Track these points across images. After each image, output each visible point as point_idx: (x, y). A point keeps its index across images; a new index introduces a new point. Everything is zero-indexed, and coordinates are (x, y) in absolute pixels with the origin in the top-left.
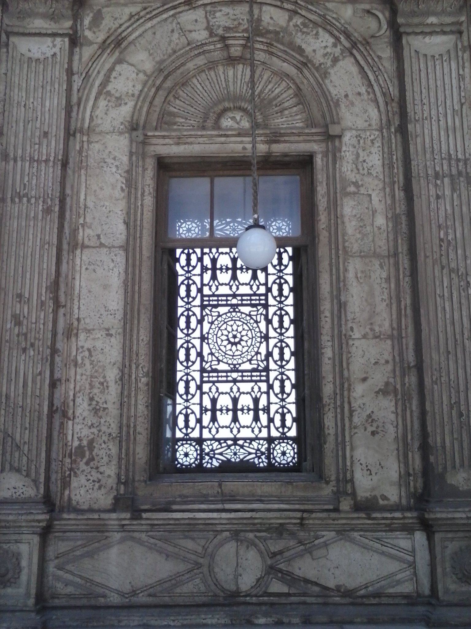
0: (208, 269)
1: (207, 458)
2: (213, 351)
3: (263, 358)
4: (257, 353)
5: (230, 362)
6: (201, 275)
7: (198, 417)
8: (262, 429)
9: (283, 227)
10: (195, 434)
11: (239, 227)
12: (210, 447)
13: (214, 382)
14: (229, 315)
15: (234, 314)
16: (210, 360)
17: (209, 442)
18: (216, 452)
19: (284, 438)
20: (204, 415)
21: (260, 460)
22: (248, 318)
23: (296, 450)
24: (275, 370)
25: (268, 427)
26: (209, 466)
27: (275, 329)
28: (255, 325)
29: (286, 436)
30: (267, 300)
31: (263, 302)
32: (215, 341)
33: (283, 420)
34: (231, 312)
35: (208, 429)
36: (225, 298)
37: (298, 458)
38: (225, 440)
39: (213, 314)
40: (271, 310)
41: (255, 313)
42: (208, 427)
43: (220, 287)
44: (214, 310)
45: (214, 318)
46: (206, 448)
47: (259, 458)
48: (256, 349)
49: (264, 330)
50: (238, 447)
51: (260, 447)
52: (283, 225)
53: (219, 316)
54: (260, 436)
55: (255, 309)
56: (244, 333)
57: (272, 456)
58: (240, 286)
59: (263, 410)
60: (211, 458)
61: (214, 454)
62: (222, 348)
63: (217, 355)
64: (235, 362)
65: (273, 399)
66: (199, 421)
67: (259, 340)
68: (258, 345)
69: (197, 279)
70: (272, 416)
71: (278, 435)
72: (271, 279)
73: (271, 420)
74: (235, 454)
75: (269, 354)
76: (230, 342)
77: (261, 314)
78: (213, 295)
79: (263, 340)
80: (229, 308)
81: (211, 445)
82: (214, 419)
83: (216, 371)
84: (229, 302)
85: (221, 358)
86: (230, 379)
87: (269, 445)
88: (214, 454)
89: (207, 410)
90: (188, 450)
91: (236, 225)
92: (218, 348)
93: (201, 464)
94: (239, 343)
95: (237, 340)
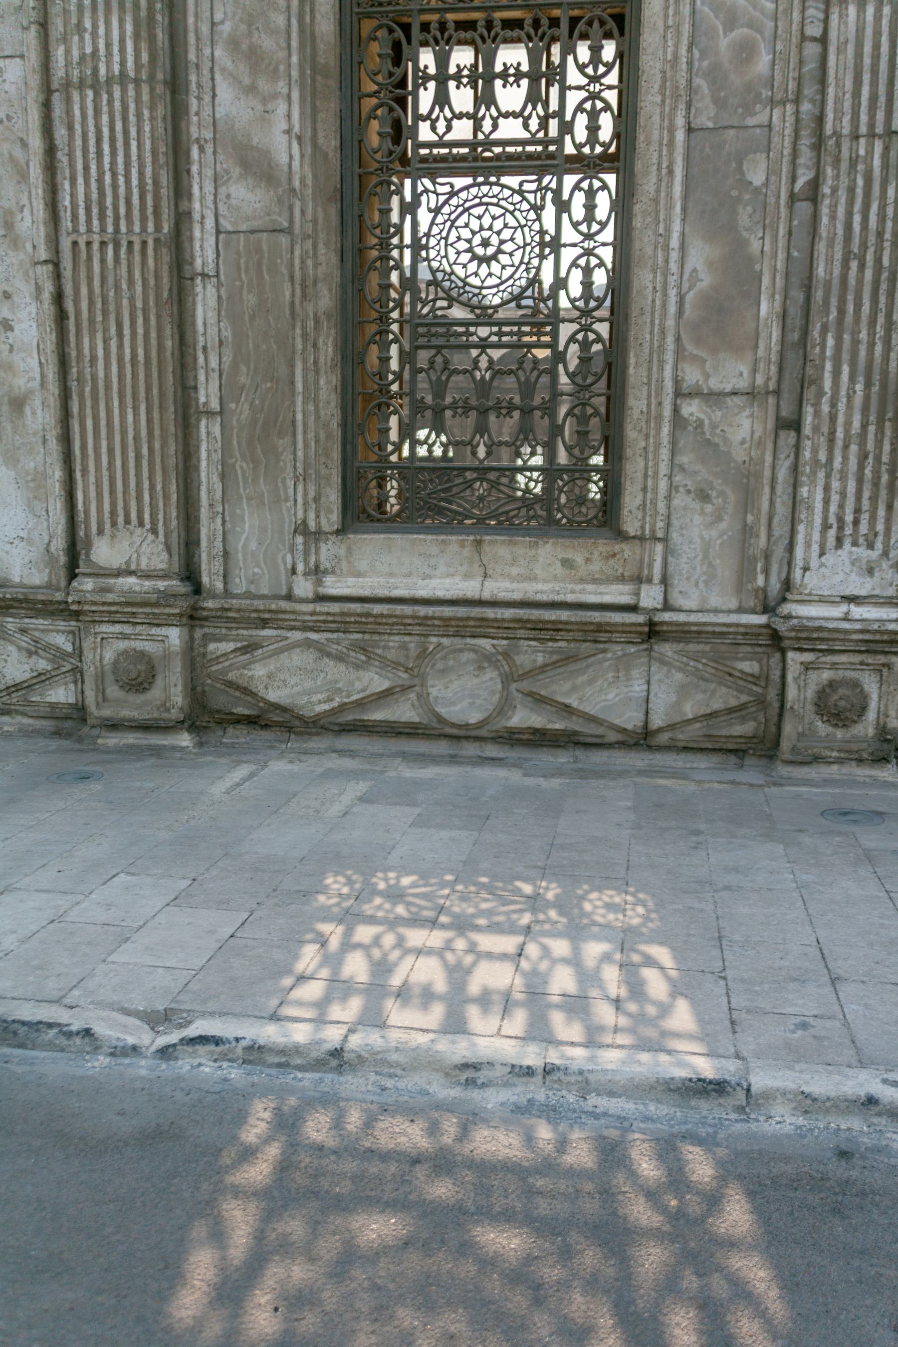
13: (439, 349)
15: (485, 189)
22: (517, 198)
28: (532, 215)
45: (442, 199)
56: (506, 234)
58: (501, 121)
68: (535, 262)
72: (573, 98)
78: (441, 144)
94: (494, 257)
95: (491, 251)
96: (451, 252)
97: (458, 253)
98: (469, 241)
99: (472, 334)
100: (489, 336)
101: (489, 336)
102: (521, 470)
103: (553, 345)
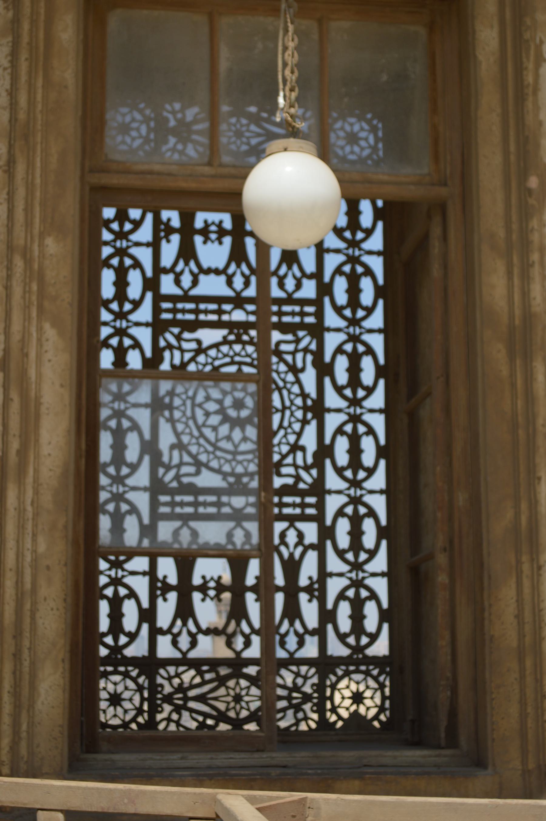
0: (173, 231)
1: (167, 708)
2: (185, 439)
3: (310, 460)
4: (295, 448)
5: (227, 468)
6: (155, 246)
7: (145, 604)
8: (307, 638)
9: (363, 134)
10: (138, 649)
11: (253, 128)
12: (176, 681)
13: (185, 519)
14: (225, 349)
15: (237, 348)
16: (176, 460)
17: (172, 670)
18: (192, 693)
19: (358, 661)
20: (160, 600)
21: (300, 715)
23: (387, 691)
24: (339, 492)
25: (320, 633)
26: (173, 727)
27: (339, 390)
28: (290, 377)
29: (366, 657)
30: (320, 314)
31: (310, 320)
32: (189, 413)
33: (357, 617)
34: (230, 343)
35: (169, 637)
36: (213, 307)
37: (391, 708)
38: (214, 663)
39: (186, 345)
40: (332, 341)
41: (291, 347)
42: (169, 631)
43: (202, 277)
44: (186, 335)
46: (166, 683)
47: (298, 708)
48: (292, 438)
49: (311, 388)
50: (244, 683)
51: (300, 681)
52: (362, 129)
53: (200, 350)
54: (302, 654)
55: (290, 337)
57: (329, 705)
59: (309, 590)
60: (178, 709)
61: (186, 699)
62: (208, 432)
63: (194, 449)
64: (239, 469)
65: (334, 563)
66: (148, 615)
67: (299, 414)
69: (145, 256)
70: (330, 605)
71: (345, 652)
73: (327, 616)
74: (238, 698)
75: (325, 451)
76: (226, 419)
77: (306, 350)
78: (186, 298)
79: (309, 415)
80: (225, 332)
81: (178, 675)
82: (185, 611)
83: (192, 490)
84: (225, 318)
85: (203, 458)
86: (226, 510)
87: (323, 678)
88: (186, 699)
89: (167, 588)
90: (120, 688)
91: (244, 121)
92: (196, 433)
93: (152, 724)
96: (199, 413)
97: (207, 414)
98: (220, 402)
99: (224, 505)
100: (244, 508)
101: (244, 508)
102: (285, 664)
103: (319, 518)
